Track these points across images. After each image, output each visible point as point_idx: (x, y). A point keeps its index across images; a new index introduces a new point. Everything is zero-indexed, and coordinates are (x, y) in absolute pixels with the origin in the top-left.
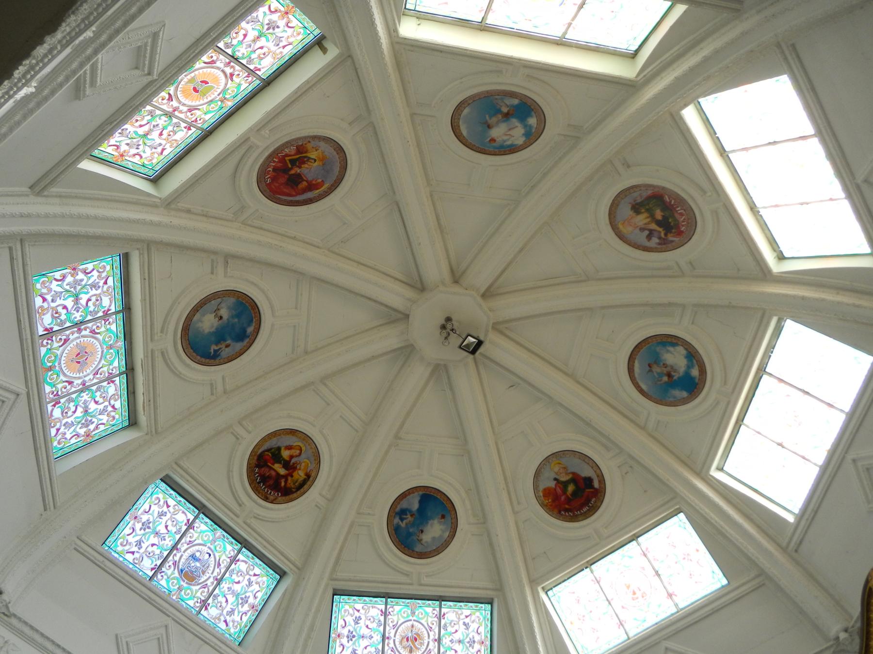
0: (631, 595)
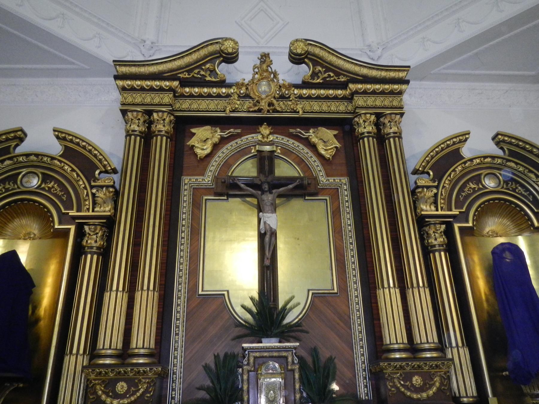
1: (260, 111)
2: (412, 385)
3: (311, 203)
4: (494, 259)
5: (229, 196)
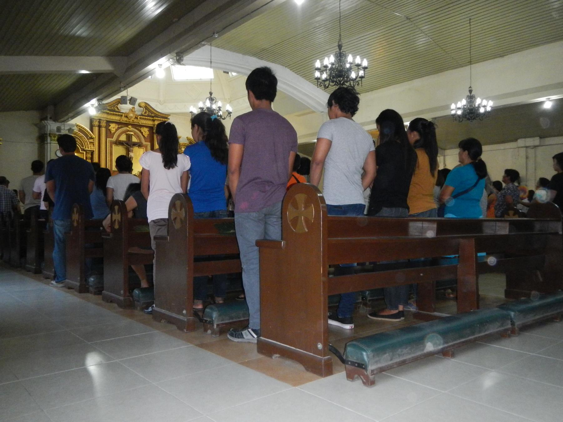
1: (130, 122)
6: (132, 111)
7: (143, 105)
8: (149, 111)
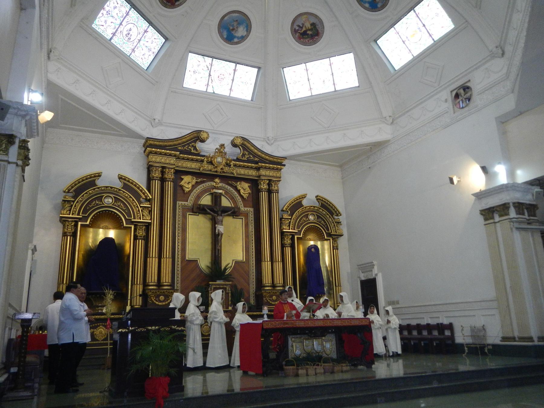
0: (127, 33)
1: (216, 171)
2: (272, 299)
3: (236, 219)
4: (308, 251)
5: (199, 213)
6: (221, 152)
7: (238, 141)
8: (250, 153)
